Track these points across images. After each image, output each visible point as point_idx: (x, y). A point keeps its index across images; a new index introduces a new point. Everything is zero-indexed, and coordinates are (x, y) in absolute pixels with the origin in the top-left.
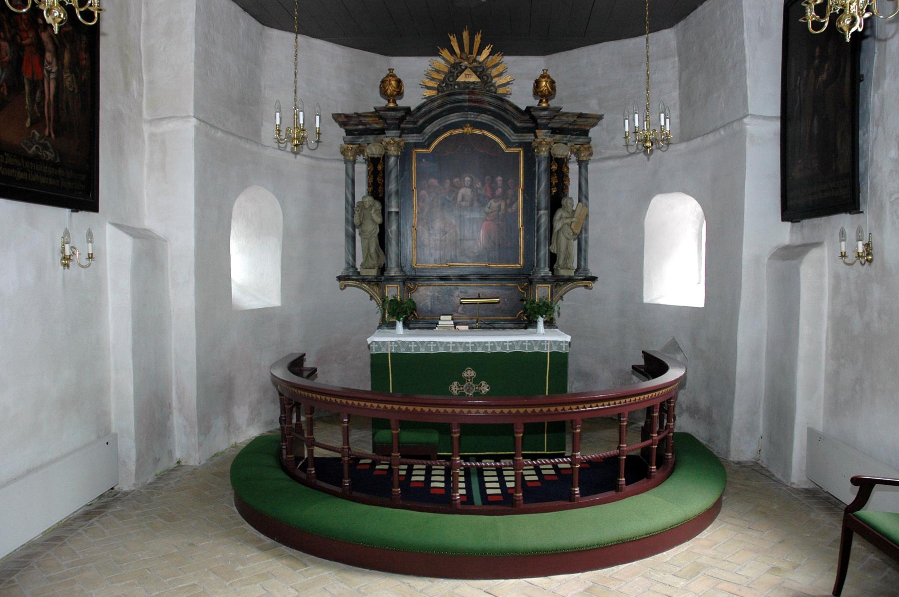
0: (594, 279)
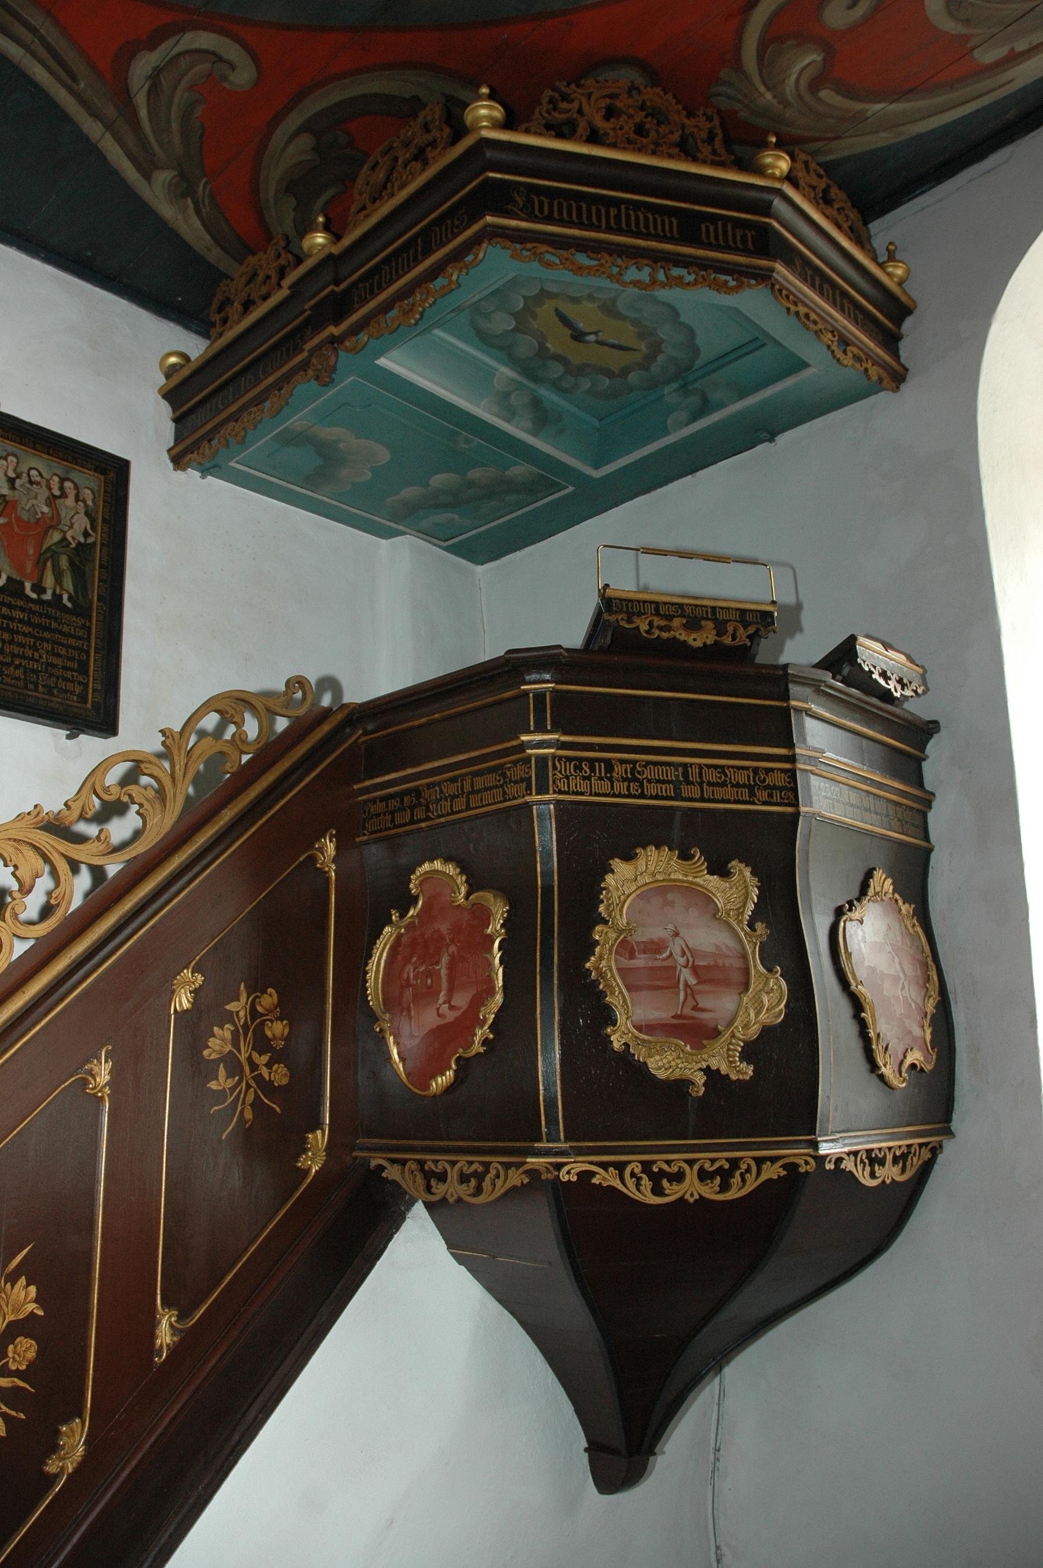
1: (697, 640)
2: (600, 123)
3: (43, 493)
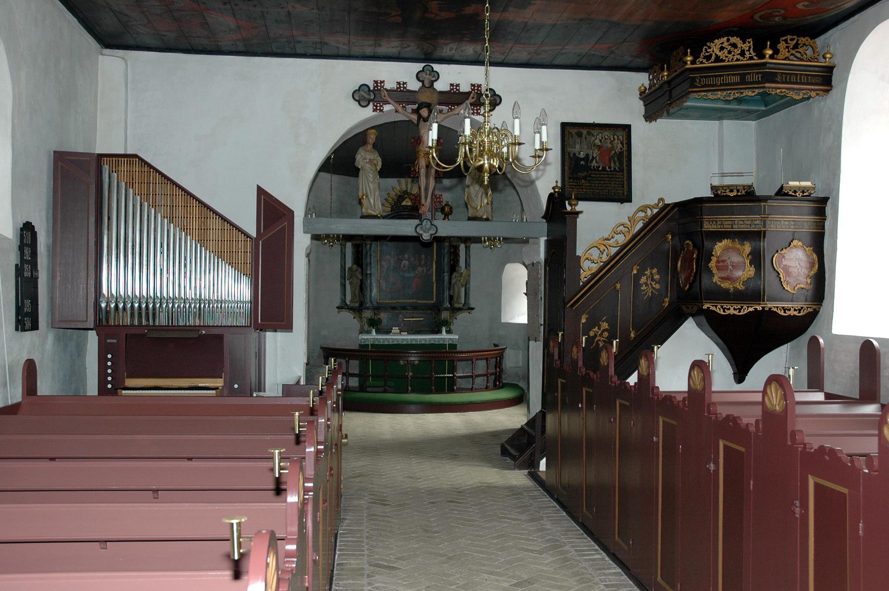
0: (473, 309)
1: (732, 194)
2: (719, 54)
3: (609, 141)
